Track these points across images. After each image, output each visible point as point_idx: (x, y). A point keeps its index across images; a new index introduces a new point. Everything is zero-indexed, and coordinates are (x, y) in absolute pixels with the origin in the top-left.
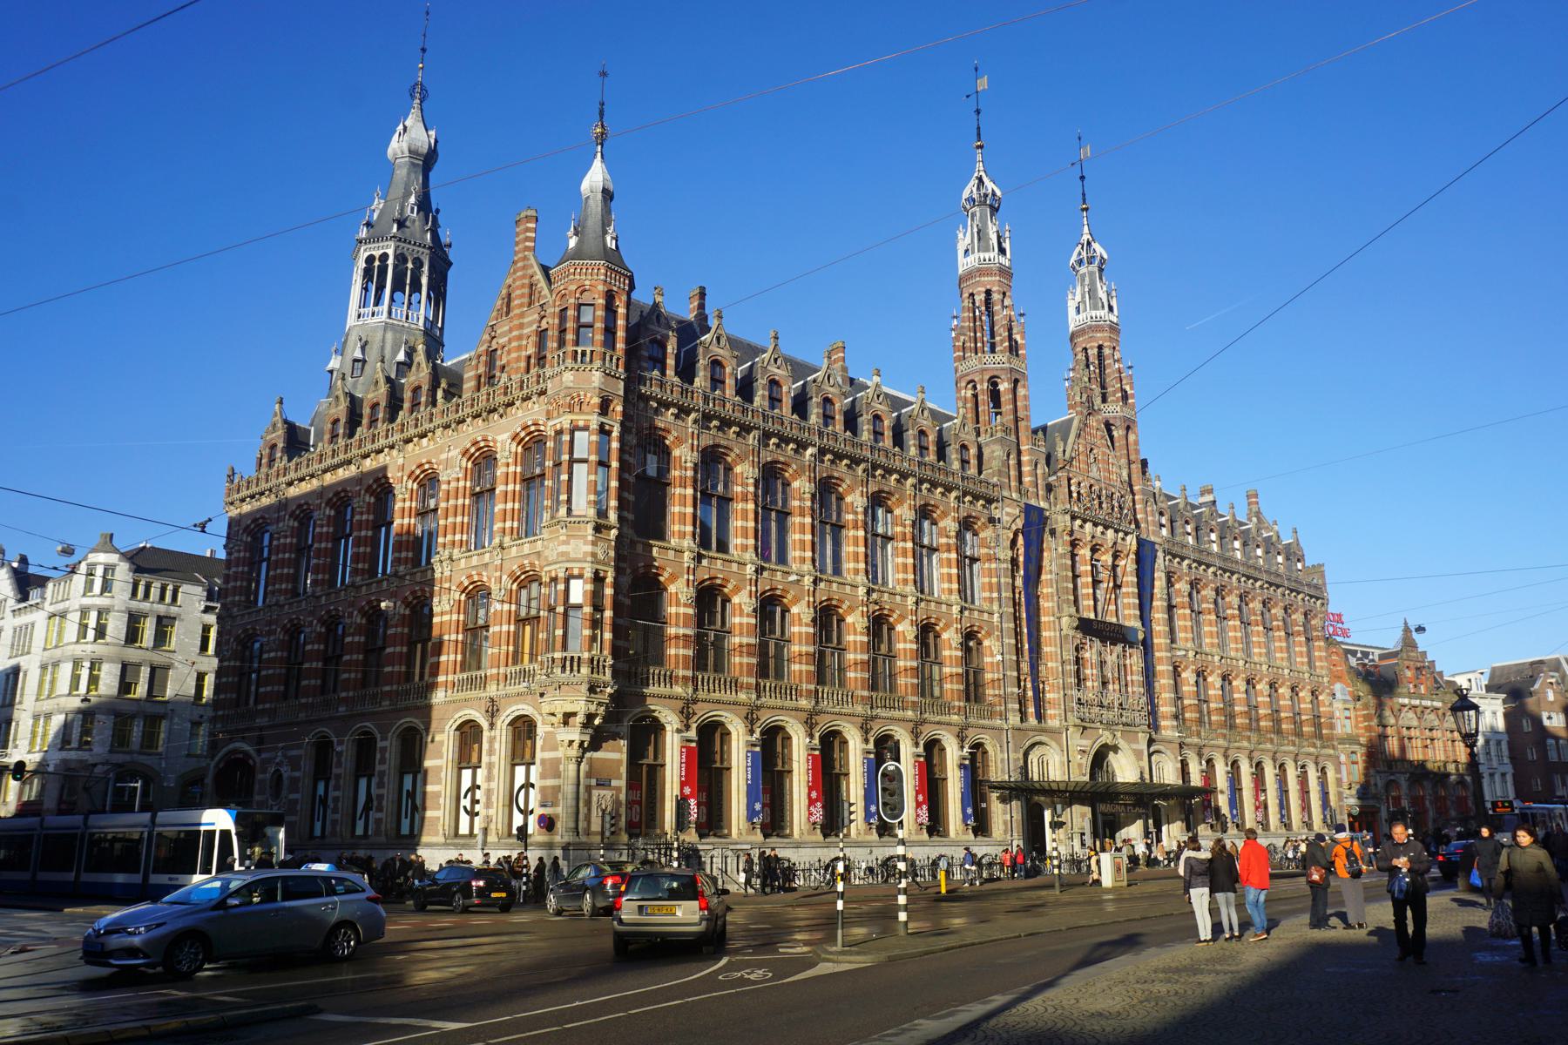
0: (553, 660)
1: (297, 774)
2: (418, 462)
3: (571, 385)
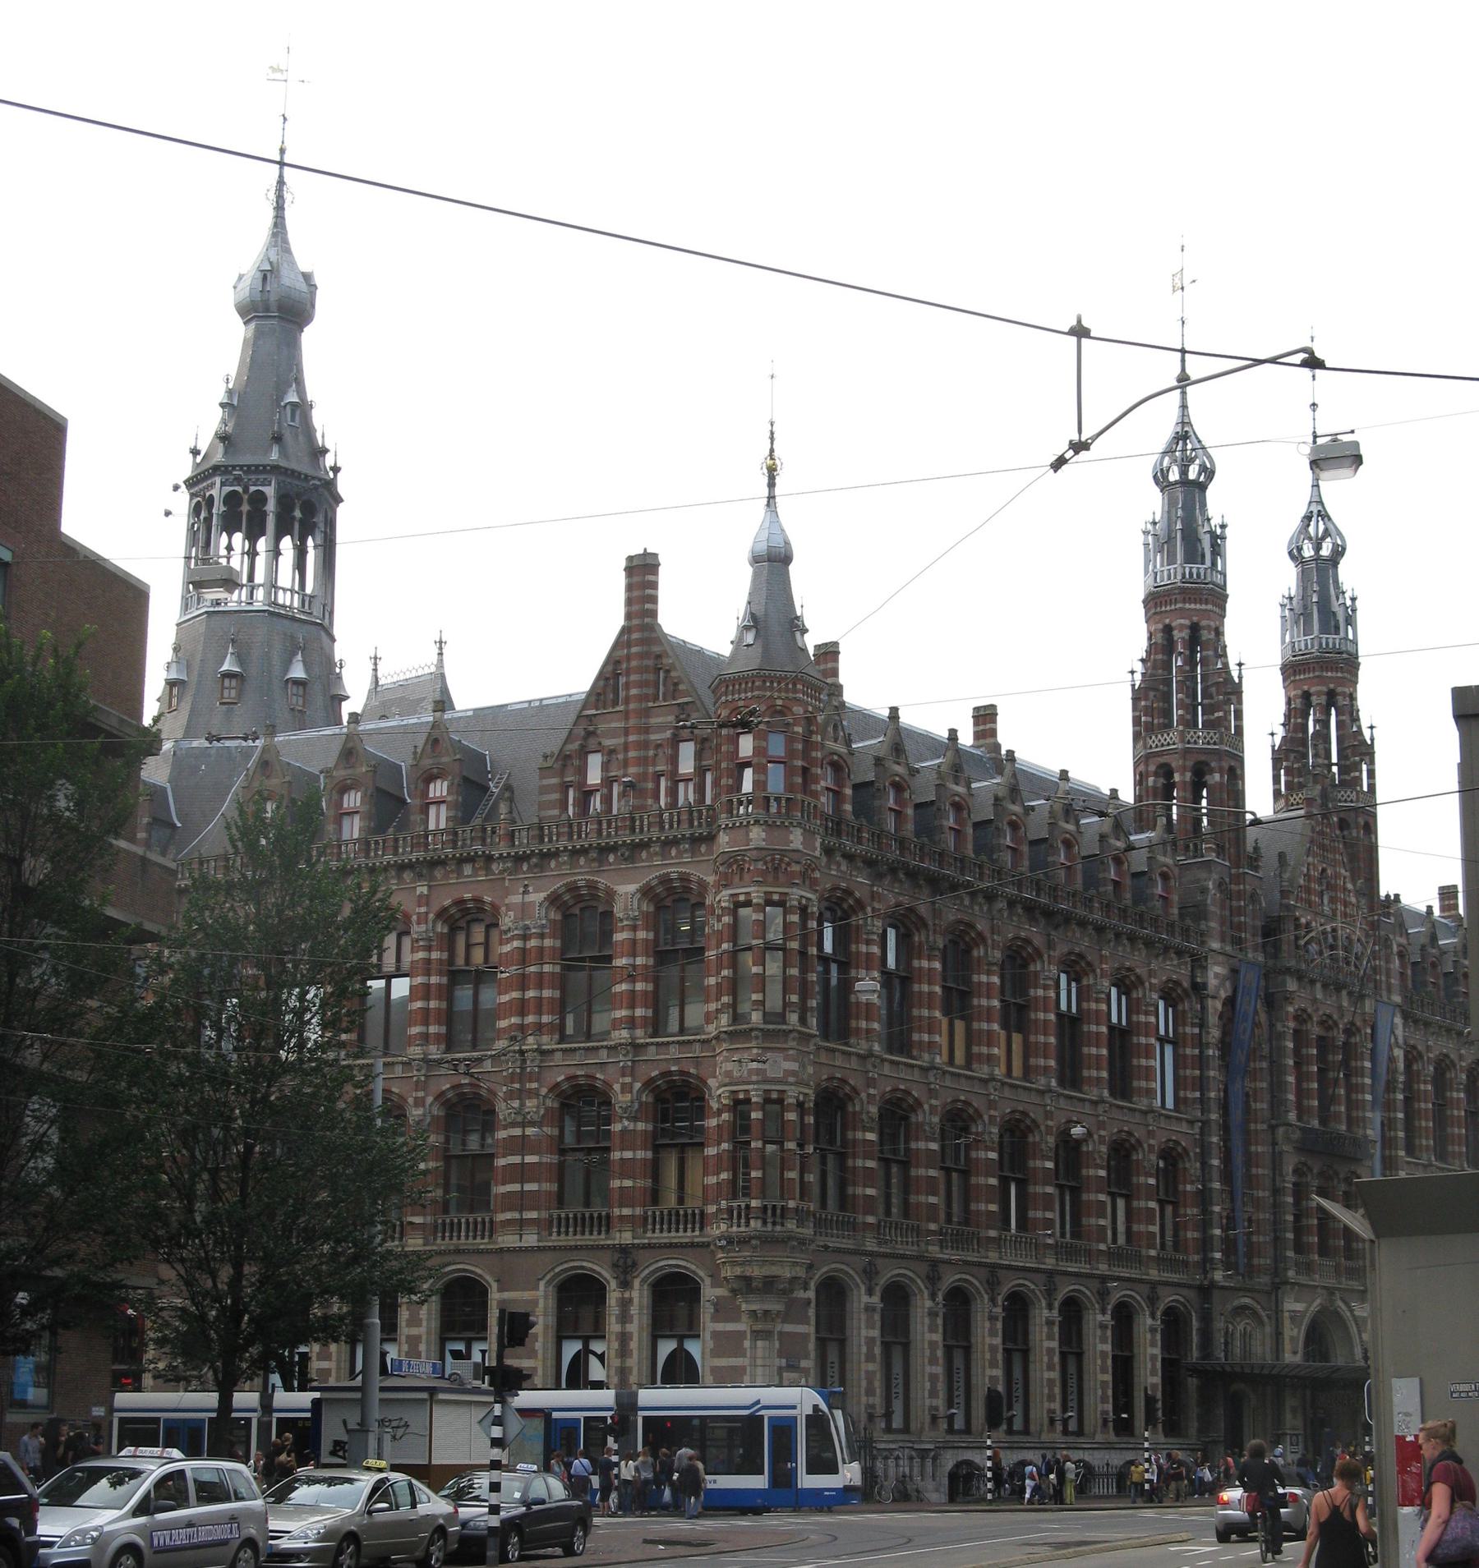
0: (748, 1207)
2: (457, 895)
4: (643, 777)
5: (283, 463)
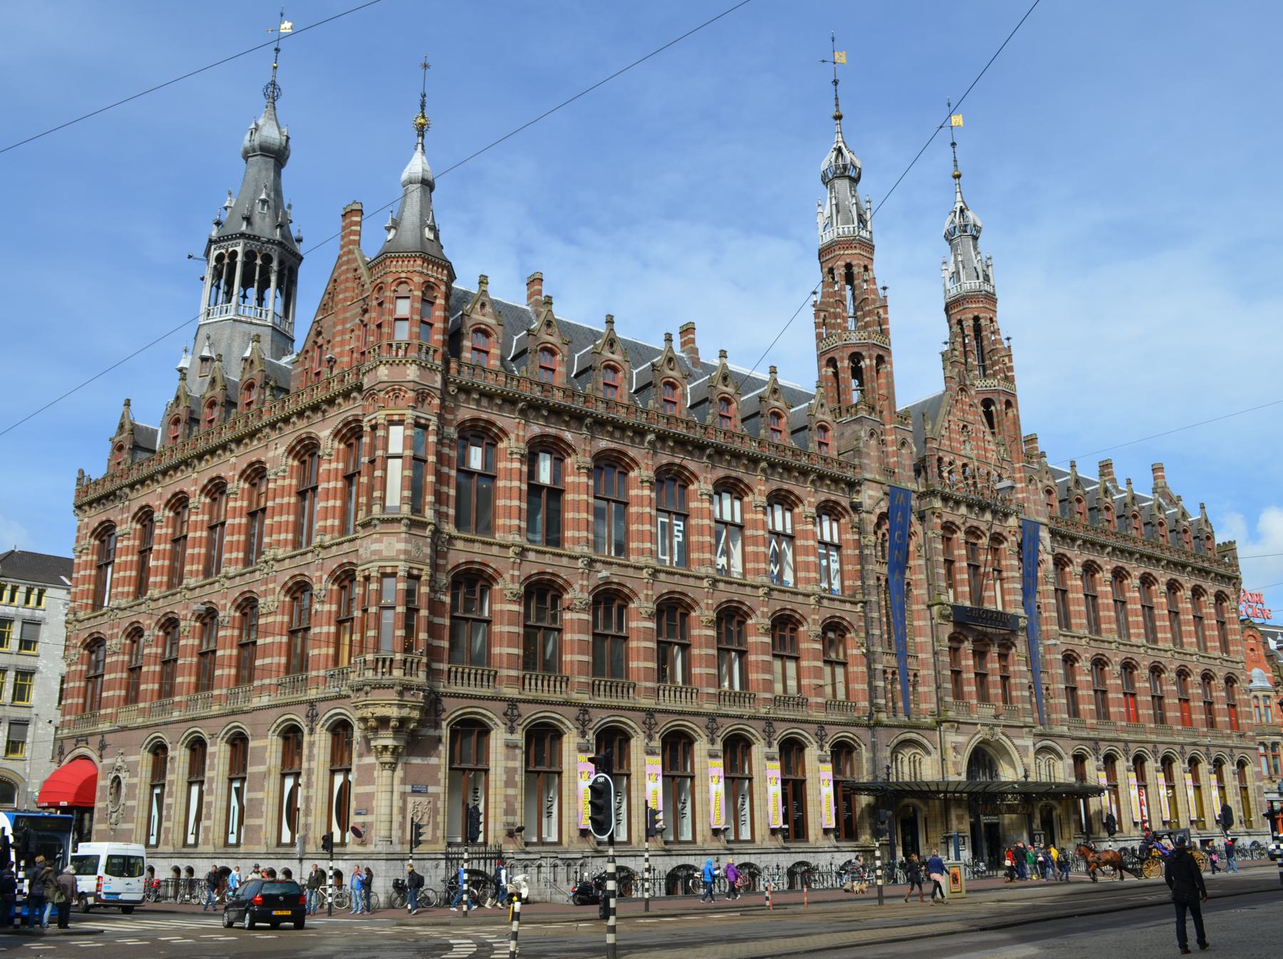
0: (365, 661)
1: (135, 780)
3: (386, 379)
4: (341, 354)
5: (249, 232)
